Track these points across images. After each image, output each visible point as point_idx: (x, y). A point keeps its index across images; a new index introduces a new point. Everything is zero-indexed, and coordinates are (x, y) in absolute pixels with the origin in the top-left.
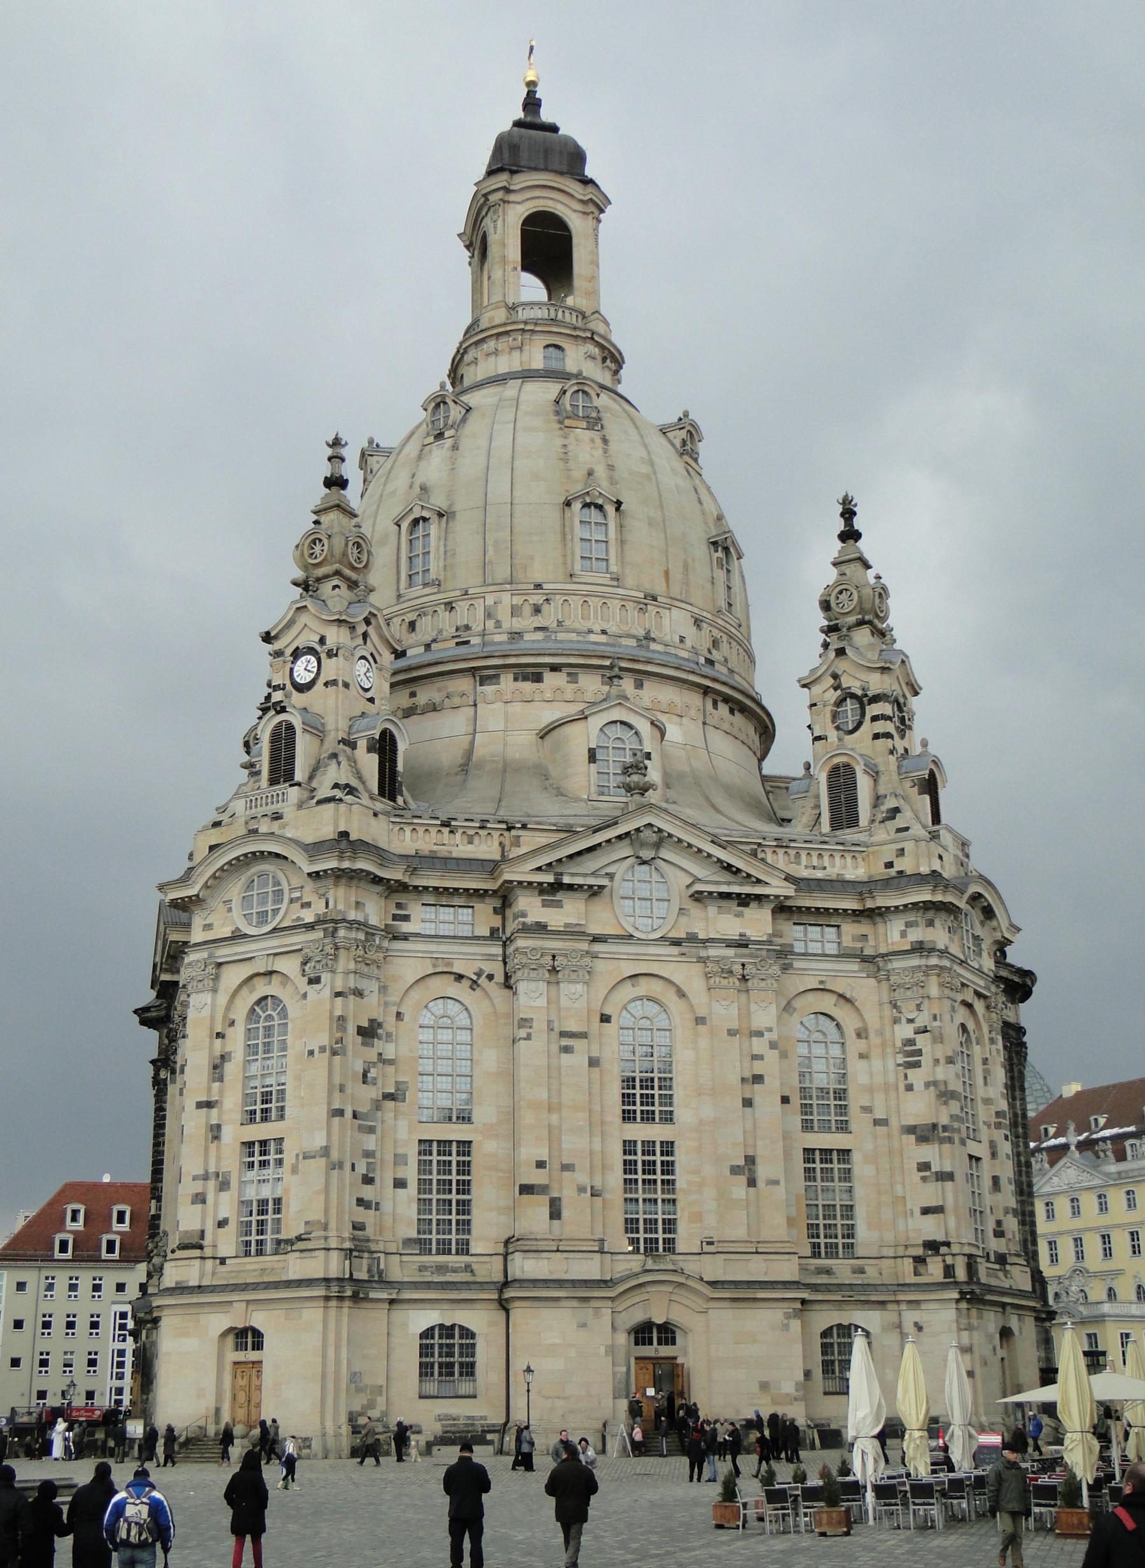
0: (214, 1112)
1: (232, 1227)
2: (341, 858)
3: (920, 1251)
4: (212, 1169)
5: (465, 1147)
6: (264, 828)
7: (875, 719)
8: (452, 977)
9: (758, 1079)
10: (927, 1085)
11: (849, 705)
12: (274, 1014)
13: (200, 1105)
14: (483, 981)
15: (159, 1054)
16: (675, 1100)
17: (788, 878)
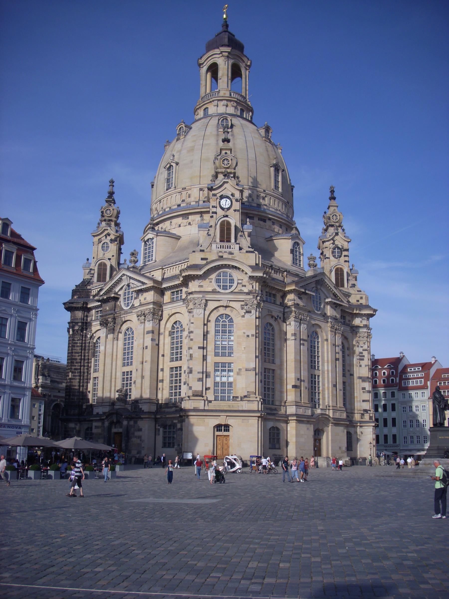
0: (205, 350)
1: (212, 391)
2: (263, 274)
3: (362, 412)
4: (205, 370)
5: (274, 370)
6: (225, 256)
7: (345, 256)
8: (271, 317)
9: (338, 359)
10: (366, 366)
11: (336, 250)
12: (227, 321)
13: (199, 348)
14: (279, 319)
15: (71, 319)
16: (320, 363)
17: (348, 302)
